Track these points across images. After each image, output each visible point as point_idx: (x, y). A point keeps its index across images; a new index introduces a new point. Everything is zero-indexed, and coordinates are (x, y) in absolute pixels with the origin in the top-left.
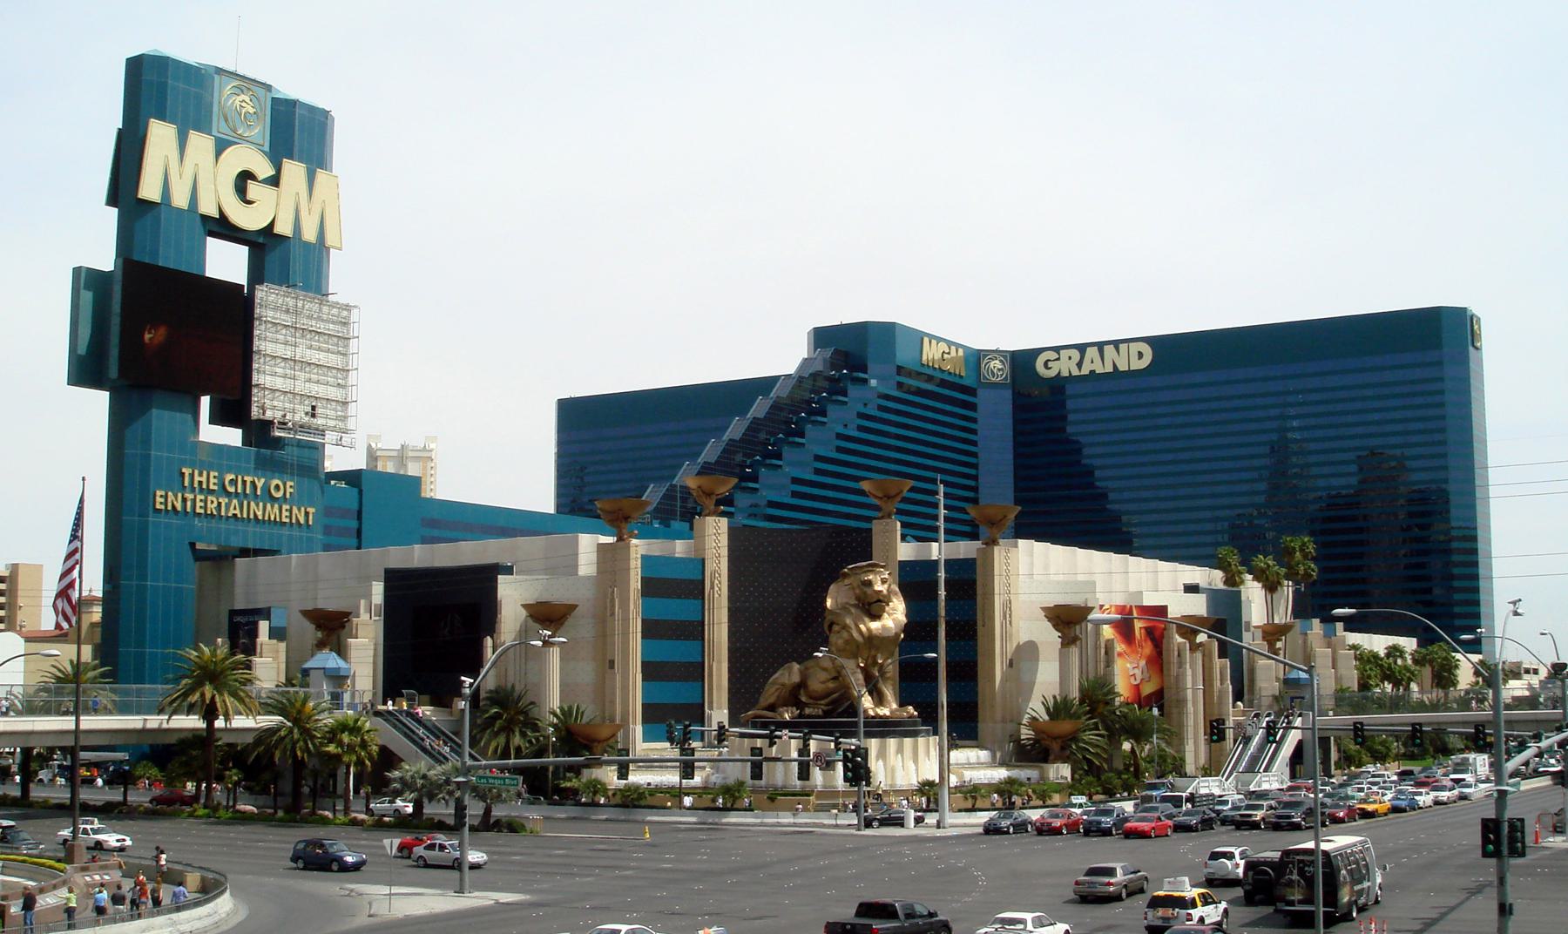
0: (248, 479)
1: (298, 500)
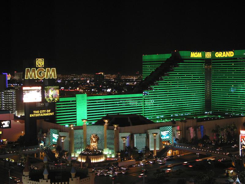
0: (43, 111)
1: (51, 112)
